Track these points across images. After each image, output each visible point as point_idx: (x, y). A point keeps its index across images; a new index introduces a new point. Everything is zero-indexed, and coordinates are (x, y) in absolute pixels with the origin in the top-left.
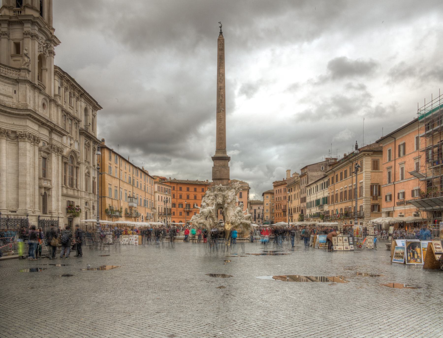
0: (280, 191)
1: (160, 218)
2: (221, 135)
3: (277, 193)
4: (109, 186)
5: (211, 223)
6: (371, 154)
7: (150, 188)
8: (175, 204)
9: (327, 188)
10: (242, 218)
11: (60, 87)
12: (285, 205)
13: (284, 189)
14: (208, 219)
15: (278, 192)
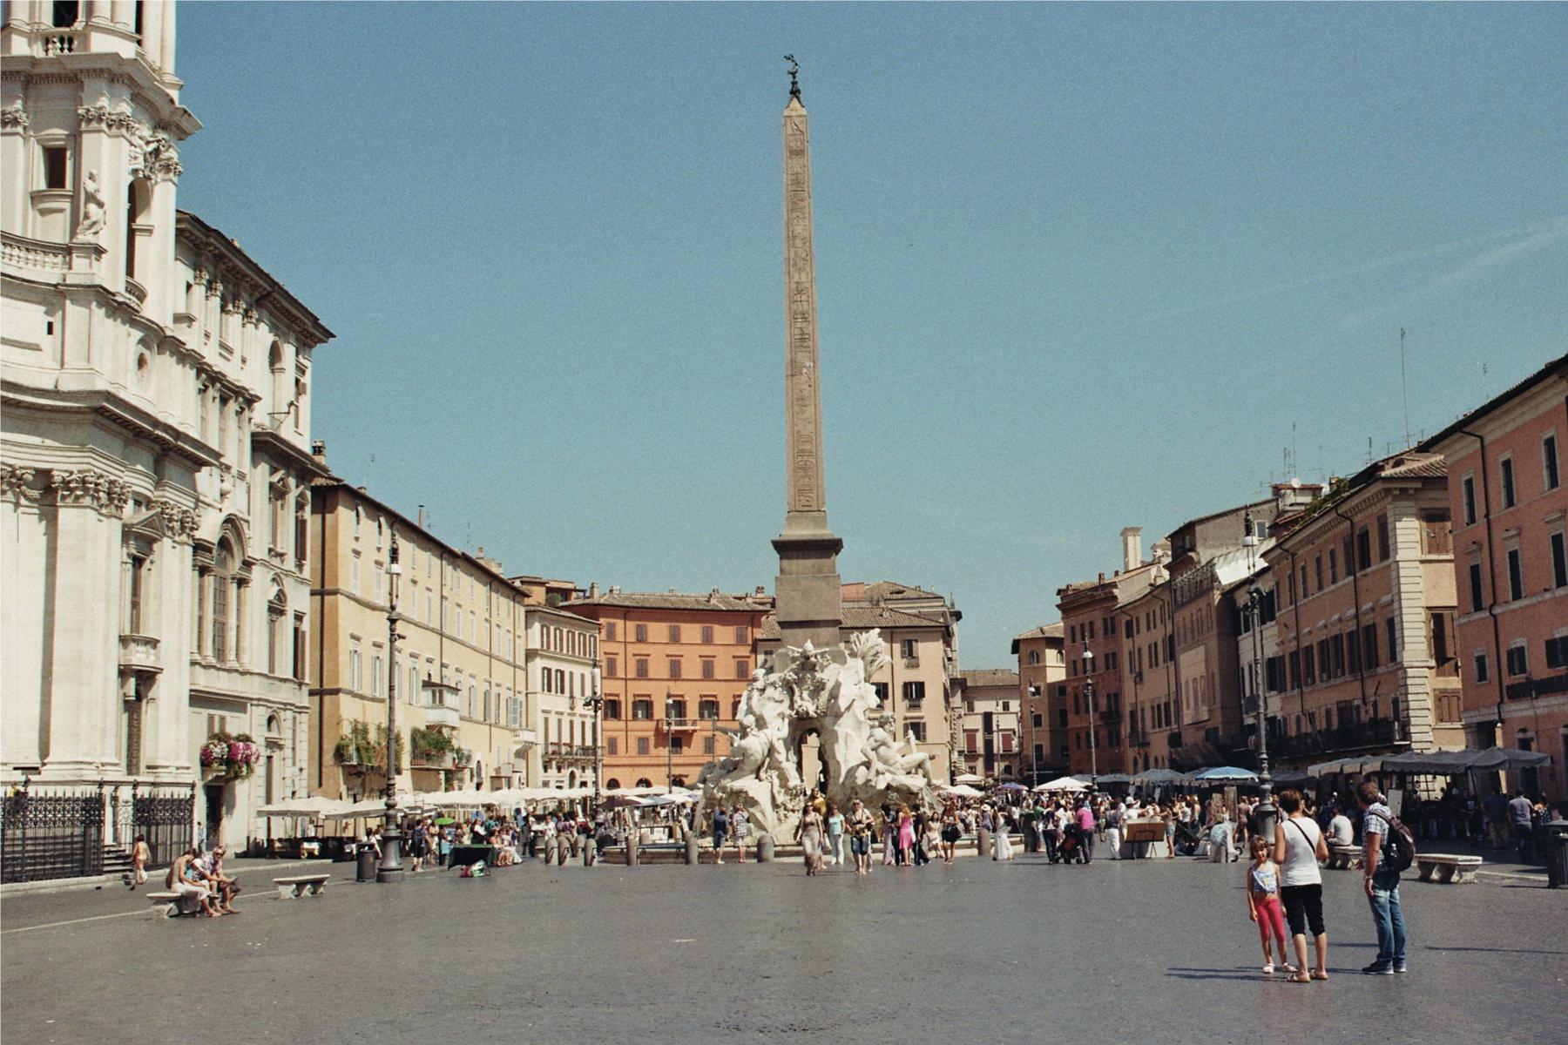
0: (1087, 628)
1: (553, 771)
2: (806, 458)
3: (1074, 641)
4: (352, 645)
5: (775, 791)
6: (1416, 489)
7: (511, 636)
8: (620, 702)
9: (1273, 623)
10: (891, 769)
11: (192, 282)
12: (1113, 691)
13: (1105, 620)
14: (762, 775)
15: (1078, 637)
